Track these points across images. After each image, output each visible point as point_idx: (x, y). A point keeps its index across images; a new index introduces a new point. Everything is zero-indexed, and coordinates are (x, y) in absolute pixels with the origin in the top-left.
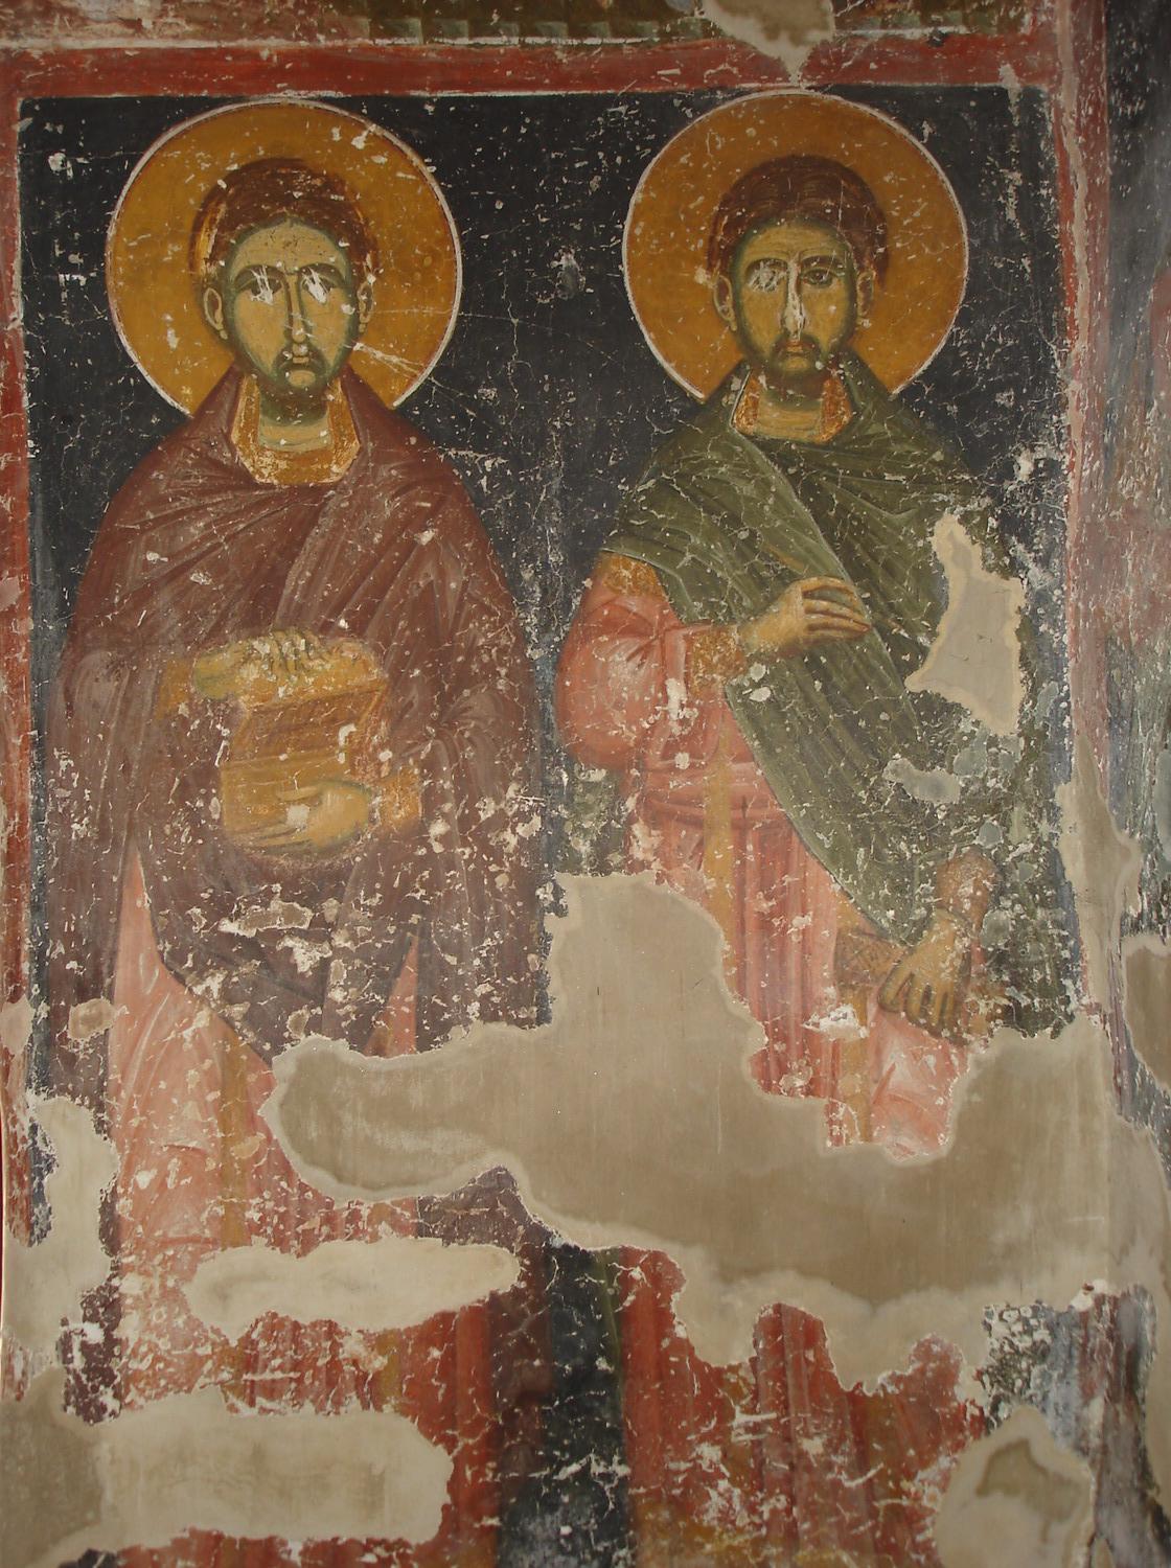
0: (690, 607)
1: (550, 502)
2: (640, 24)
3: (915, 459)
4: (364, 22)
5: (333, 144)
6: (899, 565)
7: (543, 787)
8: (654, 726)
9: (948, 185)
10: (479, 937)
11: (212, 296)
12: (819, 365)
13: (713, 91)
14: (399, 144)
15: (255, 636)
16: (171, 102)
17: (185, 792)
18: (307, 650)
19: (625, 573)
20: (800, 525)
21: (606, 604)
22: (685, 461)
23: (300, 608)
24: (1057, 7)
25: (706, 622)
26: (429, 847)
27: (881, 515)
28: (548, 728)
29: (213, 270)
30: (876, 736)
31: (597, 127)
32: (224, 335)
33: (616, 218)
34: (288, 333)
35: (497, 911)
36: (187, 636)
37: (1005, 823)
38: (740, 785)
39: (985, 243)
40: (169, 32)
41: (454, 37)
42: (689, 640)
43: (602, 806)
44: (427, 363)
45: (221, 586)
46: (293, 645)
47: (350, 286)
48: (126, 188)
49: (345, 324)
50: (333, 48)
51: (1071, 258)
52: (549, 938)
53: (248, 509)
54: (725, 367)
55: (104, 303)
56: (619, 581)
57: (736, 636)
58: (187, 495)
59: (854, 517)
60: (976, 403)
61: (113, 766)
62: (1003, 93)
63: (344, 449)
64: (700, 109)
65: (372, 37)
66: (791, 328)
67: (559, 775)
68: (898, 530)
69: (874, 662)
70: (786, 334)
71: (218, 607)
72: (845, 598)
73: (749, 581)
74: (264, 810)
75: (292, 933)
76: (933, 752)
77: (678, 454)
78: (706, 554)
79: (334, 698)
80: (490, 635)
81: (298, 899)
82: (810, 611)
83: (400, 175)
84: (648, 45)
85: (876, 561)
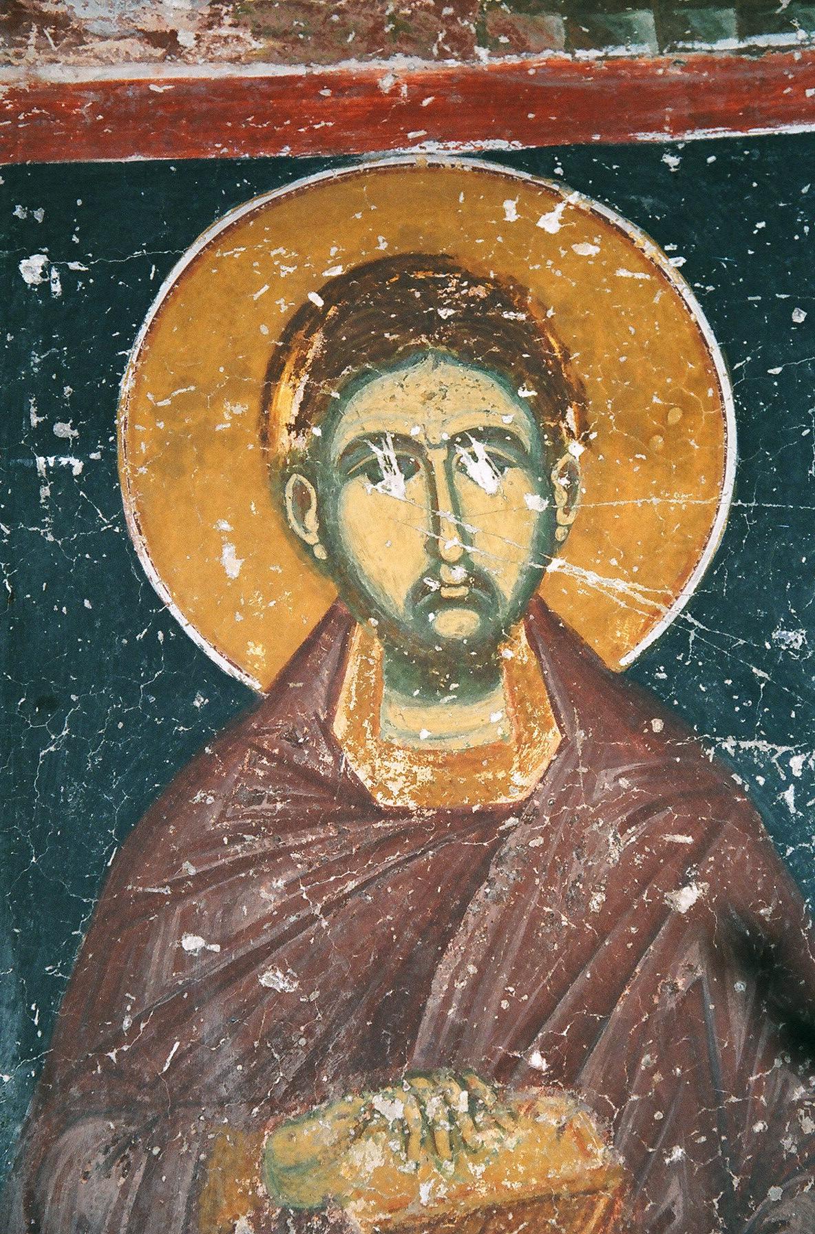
4: (556, 21)
5: (506, 228)
14: (621, 222)
15: (375, 1086)
16: (228, 167)
18: (472, 1112)
23: (458, 1031)
29: (301, 444)
32: (320, 553)
36: (251, 1091)
40: (224, 52)
41: (711, 38)
45: (315, 995)
46: (446, 1102)
47: (541, 464)
48: (153, 310)
49: (530, 529)
50: (504, 70)
53: (365, 853)
55: (114, 504)
58: (255, 831)
63: (533, 744)
65: (568, 48)
71: (309, 1033)
79: (523, 1204)
83: (622, 273)
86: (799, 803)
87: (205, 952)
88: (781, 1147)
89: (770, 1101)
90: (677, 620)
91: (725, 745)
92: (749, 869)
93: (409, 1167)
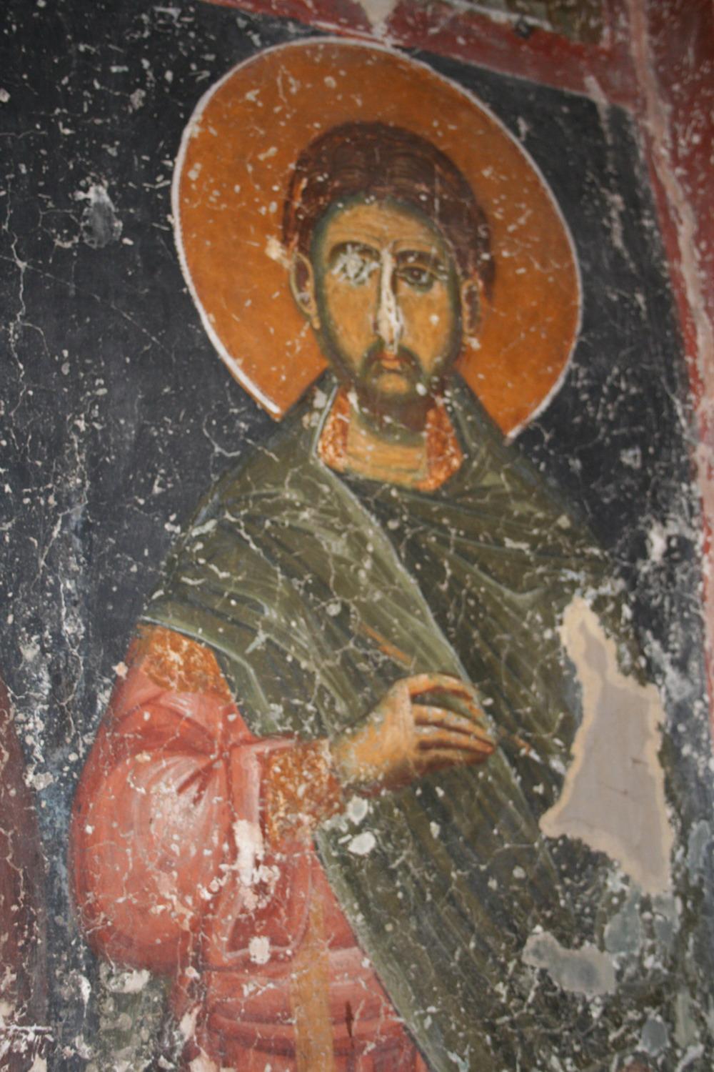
0: (266, 712)
1: (65, 540)
3: (539, 523)
6: (524, 661)
8: (217, 897)
9: (550, 195)
12: (421, 389)
13: (284, 21)
19: (173, 662)
20: (403, 600)
21: (147, 703)
22: (256, 498)
24: (632, 28)
25: (288, 735)
27: (501, 594)
28: (59, 905)
30: (510, 900)
31: (140, 26)
33: (164, 151)
37: (669, 1018)
38: (342, 984)
39: (597, 269)
42: (265, 762)
43: (145, 1034)
51: (685, 302)
54: (306, 376)
56: (166, 669)
57: (327, 756)
59: (470, 595)
60: (600, 462)
62: (592, 106)
64: (272, 38)
66: (384, 332)
67: (76, 984)
68: (521, 613)
69: (501, 795)
70: (380, 344)
72: (463, 704)
73: (343, 674)
76: (580, 923)
77: (246, 488)
78: (285, 634)
82: (421, 722)
85: (498, 654)
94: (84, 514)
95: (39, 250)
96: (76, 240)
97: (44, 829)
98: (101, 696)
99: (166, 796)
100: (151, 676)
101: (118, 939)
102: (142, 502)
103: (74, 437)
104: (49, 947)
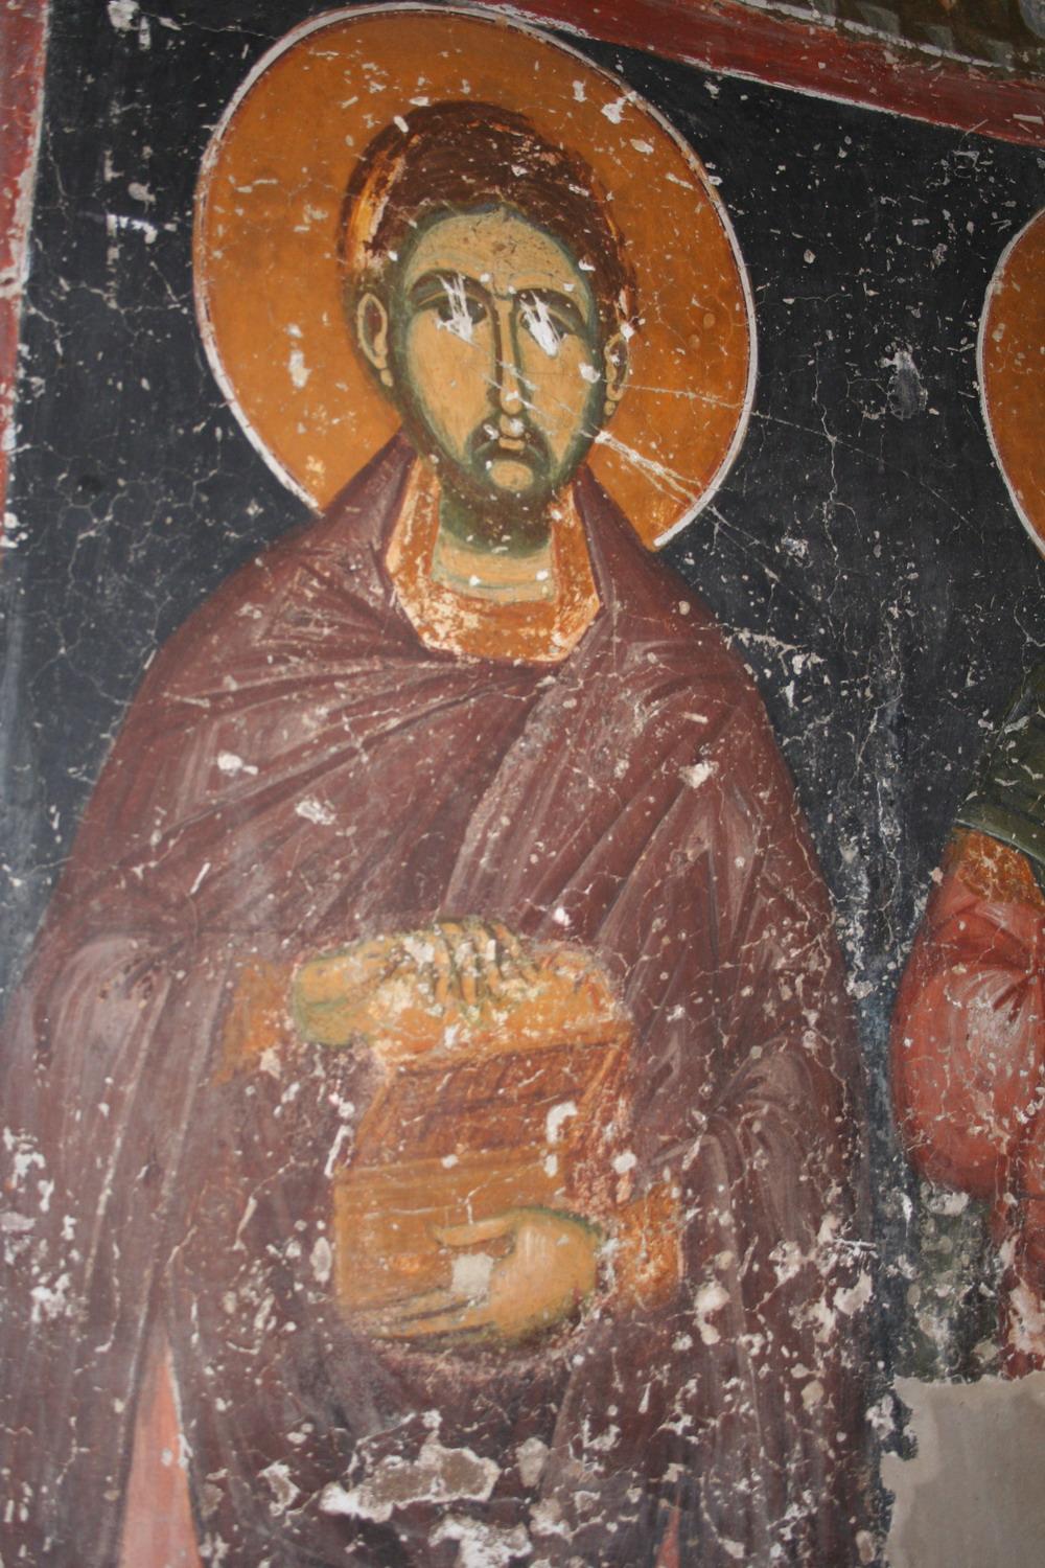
1: (879, 734)
2: (990, 42)
5: (575, 106)
7: (867, 1220)
10: (778, 1504)
11: (371, 310)
14: (671, 131)
15: (407, 927)
17: (267, 1228)
18: (499, 962)
21: (965, 911)
23: (489, 881)
26: (696, 1335)
28: (880, 1119)
29: (376, 264)
31: (939, 173)
32: (387, 379)
34: (494, 395)
35: (806, 1452)
43: (965, 1258)
44: (706, 481)
45: (351, 831)
46: (475, 949)
47: (597, 337)
48: (242, 91)
49: (584, 396)
52: (888, 1499)
53: (409, 692)
55: (185, 285)
56: (980, 875)
58: (300, 653)
61: (124, 1172)
63: (574, 607)
67: (899, 1203)
71: (344, 868)
74: (410, 1265)
75: (459, 1510)
79: (540, 1052)
80: (794, 953)
81: (472, 1441)
83: (671, 177)
84: (999, 74)
86: (797, 698)
87: (241, 774)
88: (763, 1010)
89: (757, 967)
90: (704, 511)
91: (741, 636)
92: (752, 753)
93: (435, 1011)
94: (899, 709)
95: (847, 423)
96: (884, 411)
97: (865, 1039)
98: (917, 902)
99: (983, 1011)
100: (966, 883)
101: (937, 1158)
102: (955, 695)
103: (889, 625)
104: (872, 1162)
